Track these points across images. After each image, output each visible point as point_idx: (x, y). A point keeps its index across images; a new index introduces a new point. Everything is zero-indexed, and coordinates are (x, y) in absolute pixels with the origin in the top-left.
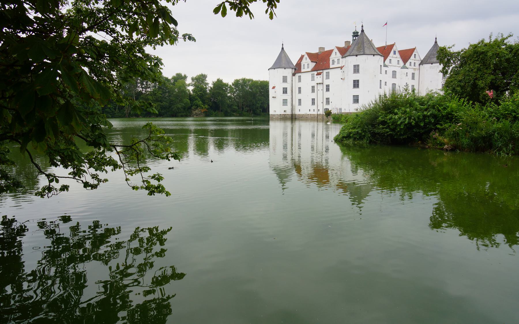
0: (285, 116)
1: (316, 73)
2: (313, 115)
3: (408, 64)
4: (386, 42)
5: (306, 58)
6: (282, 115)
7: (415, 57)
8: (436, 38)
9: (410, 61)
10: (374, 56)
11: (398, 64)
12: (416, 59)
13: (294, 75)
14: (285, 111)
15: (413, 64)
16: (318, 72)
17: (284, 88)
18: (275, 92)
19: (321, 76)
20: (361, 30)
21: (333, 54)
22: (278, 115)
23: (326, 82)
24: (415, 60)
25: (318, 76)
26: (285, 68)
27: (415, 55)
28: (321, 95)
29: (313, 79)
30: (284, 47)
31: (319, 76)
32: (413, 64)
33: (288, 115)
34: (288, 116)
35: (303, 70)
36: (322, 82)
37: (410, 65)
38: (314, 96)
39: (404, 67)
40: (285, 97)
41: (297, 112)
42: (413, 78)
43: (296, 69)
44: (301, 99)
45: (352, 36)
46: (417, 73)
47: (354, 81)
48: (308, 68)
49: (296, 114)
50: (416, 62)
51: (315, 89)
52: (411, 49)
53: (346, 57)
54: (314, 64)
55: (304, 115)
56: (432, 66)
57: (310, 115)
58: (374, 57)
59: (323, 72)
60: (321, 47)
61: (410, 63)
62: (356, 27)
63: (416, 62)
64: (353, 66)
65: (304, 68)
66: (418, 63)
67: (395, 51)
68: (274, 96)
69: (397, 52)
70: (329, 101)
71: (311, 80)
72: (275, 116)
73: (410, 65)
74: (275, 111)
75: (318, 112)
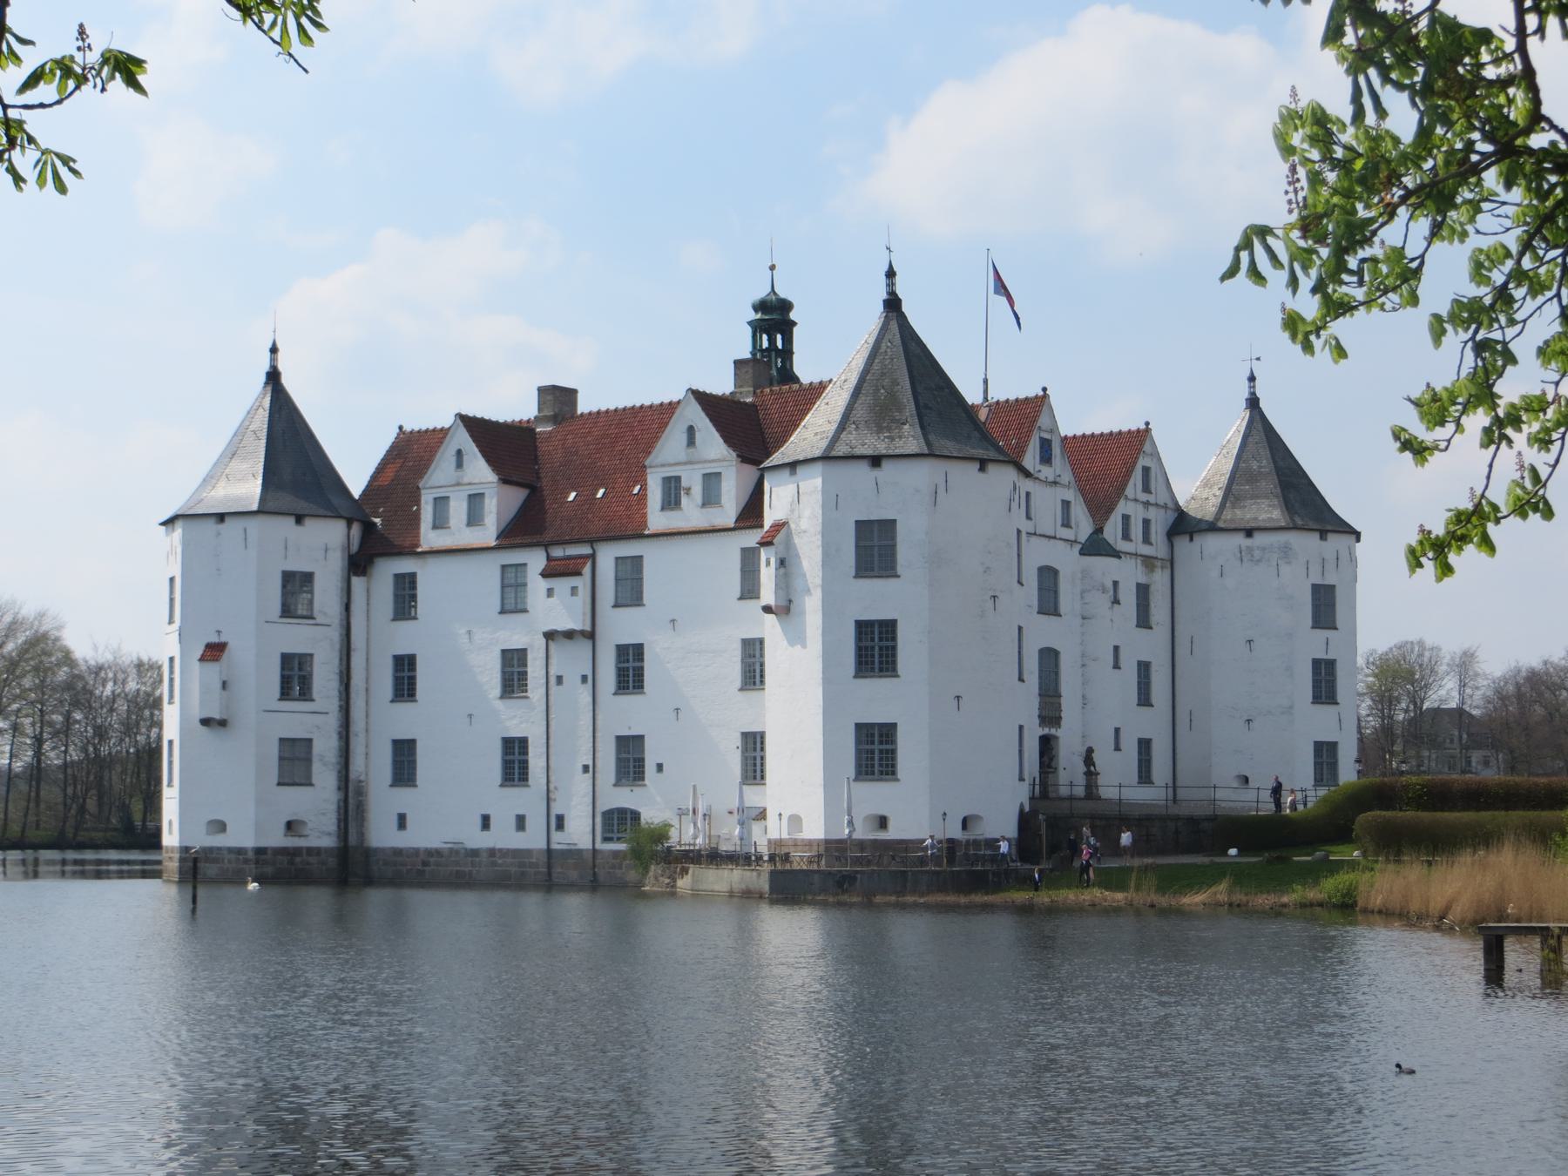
0: (291, 863)
1: (535, 561)
2: (516, 853)
3: (1112, 531)
4: (986, 381)
5: (459, 453)
6: (269, 856)
7: (1146, 488)
8: (1252, 379)
9: (1122, 507)
10: (982, 469)
11: (1066, 524)
12: (1152, 499)
13: (359, 563)
14: (290, 825)
15: (1136, 530)
16: (557, 552)
17: (286, 659)
18: (224, 685)
19: (582, 583)
20: (884, 296)
22: (240, 851)
23: (621, 626)
26: (299, 520)
27: (1146, 470)
29: (512, 602)
30: (280, 368)
31: (563, 585)
32: (1136, 530)
33: (316, 851)
34: (313, 860)
35: (430, 538)
36: (588, 628)
37: (1126, 536)
38: (521, 719)
39: (1096, 546)
40: (296, 721)
41: (382, 834)
42: (1144, 621)
43: (374, 524)
44: (412, 742)
45: (749, 331)
46: (1160, 580)
47: (863, 628)
48: (474, 519)
49: (383, 850)
50: (1152, 514)
51: (529, 670)
52: (1120, 433)
53: (800, 470)
54: (517, 496)
55: (437, 853)
56: (1250, 549)
57: (492, 852)
58: (981, 475)
59: (593, 557)
60: (555, 387)
61: (1126, 518)
62: (772, 268)
63: (1152, 514)
64: (852, 527)
65: (440, 523)
66: (1160, 522)
68: (217, 716)
69: (1056, 450)
70: (642, 760)
71: (499, 609)
72: (215, 861)
73: (1126, 536)
74: (220, 827)
75: (557, 837)
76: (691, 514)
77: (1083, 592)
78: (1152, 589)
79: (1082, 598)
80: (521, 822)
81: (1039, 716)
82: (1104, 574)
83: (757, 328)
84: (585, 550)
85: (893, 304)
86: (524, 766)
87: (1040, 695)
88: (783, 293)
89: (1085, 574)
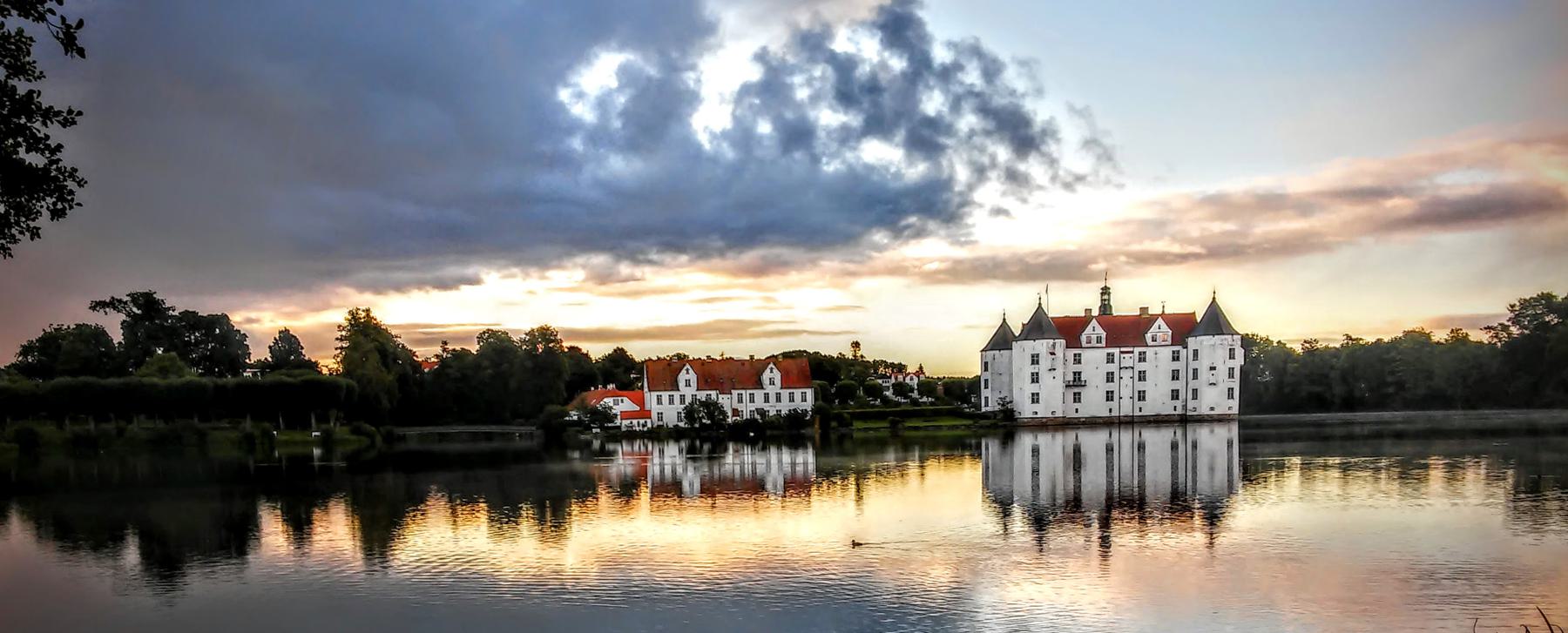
1: (1116, 351)
21: (1156, 324)
25: (1122, 356)
28: (1126, 387)
76: (1159, 341)
80: (1110, 411)
83: (1102, 294)
84: (1131, 349)
86: (1112, 397)
88: (1108, 286)
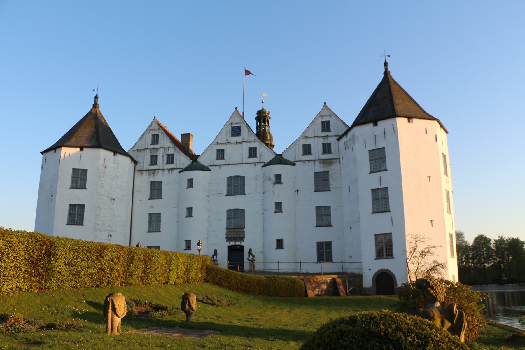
24: (328, 136)
67: (239, 128)
77: (263, 182)
78: (330, 173)
79: (263, 185)
81: (226, 238)
82: (269, 173)
85: (95, 105)
87: (227, 229)
89: (264, 174)
